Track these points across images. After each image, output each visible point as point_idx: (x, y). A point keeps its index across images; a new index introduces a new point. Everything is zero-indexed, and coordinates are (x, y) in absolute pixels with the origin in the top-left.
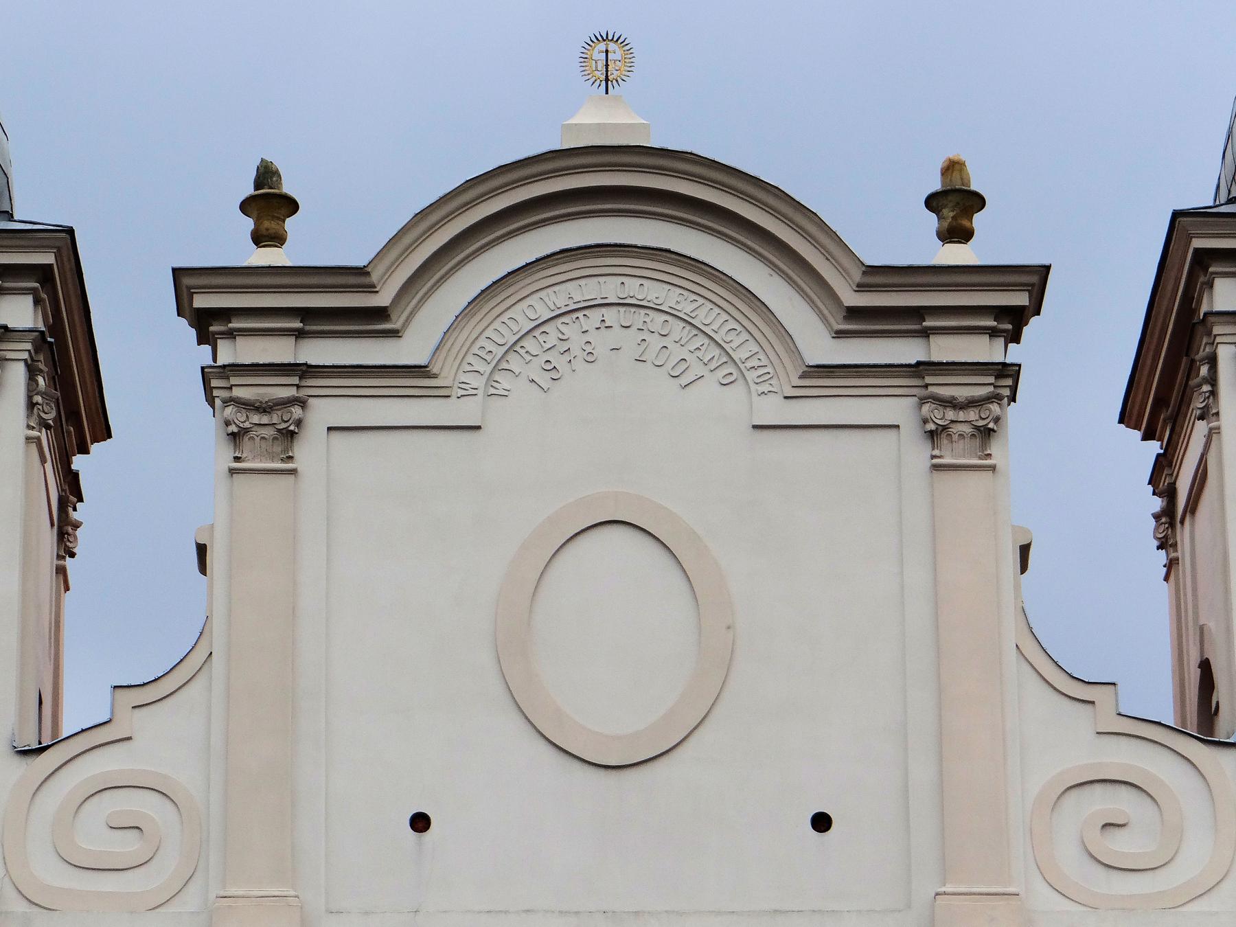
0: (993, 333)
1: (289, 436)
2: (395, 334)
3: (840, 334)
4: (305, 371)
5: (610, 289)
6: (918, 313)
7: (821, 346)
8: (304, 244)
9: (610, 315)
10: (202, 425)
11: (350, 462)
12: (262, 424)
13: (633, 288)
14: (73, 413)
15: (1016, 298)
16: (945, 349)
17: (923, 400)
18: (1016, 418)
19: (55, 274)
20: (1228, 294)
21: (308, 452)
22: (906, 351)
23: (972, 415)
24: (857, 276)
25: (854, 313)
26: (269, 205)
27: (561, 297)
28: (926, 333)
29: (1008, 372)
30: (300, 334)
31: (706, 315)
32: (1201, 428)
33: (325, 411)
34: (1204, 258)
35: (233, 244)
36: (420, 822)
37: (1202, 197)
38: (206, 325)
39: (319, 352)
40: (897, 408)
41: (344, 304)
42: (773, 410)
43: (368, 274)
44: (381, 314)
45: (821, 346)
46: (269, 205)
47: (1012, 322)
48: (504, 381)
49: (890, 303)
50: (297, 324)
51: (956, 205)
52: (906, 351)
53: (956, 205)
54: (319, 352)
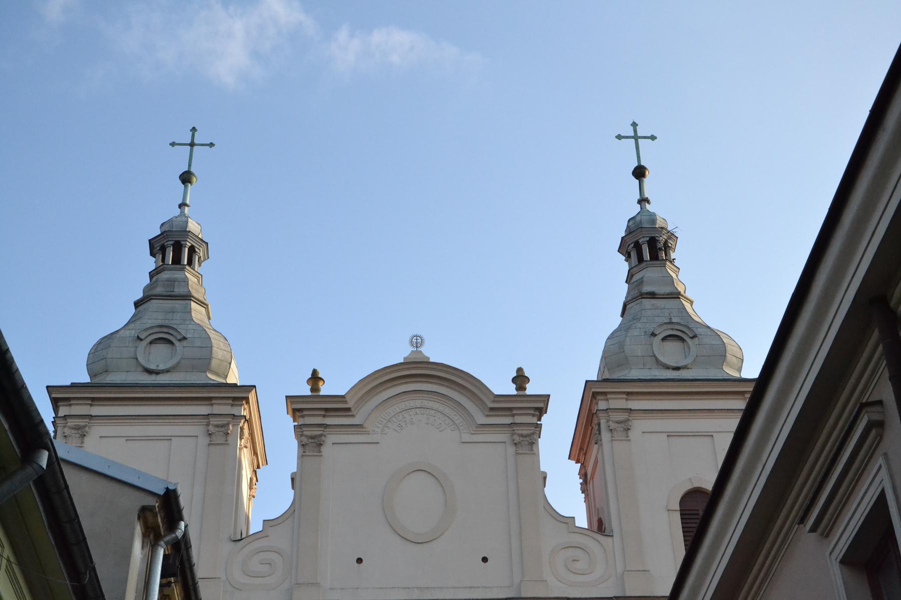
0: (533, 415)
1: (320, 445)
2: (353, 416)
3: (487, 416)
4: (326, 426)
5: (418, 403)
6: (510, 409)
7: (481, 419)
8: (325, 390)
9: (418, 411)
10: (292, 445)
11: (337, 452)
13: (426, 403)
15: (540, 406)
16: (518, 419)
17: (513, 435)
18: (541, 441)
20: (602, 405)
21: (326, 450)
23: (528, 439)
24: (492, 398)
25: (492, 409)
26: (315, 379)
28: (513, 415)
30: (324, 416)
31: (447, 411)
32: (596, 446)
33: (331, 438)
34: (595, 395)
36: (359, 561)
40: (504, 437)
41: (337, 406)
42: (466, 437)
43: (346, 402)
44: (349, 409)
45: (481, 419)
46: (315, 379)
48: (386, 430)
49: (501, 406)
50: (323, 413)
51: (520, 379)
52: (508, 420)
53: (520, 379)
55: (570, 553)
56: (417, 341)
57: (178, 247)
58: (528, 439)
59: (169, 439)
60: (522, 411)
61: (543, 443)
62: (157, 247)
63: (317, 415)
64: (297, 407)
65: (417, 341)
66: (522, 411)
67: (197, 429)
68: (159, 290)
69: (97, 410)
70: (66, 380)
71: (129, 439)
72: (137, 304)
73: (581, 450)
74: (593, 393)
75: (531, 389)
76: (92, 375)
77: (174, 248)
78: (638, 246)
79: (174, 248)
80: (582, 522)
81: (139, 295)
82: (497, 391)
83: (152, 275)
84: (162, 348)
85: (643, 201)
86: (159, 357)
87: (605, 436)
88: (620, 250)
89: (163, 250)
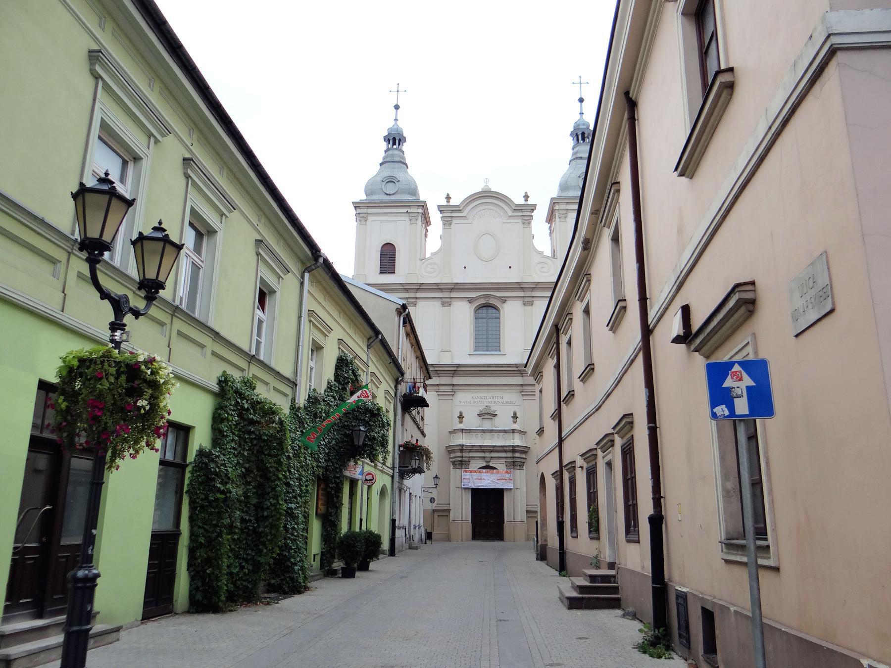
7: (510, 213)
8: (452, 203)
10: (441, 223)
11: (456, 225)
12: (447, 223)
14: (427, 222)
15: (533, 208)
16: (524, 214)
18: (533, 222)
19: (424, 206)
20: (557, 207)
21: (453, 226)
22: (520, 214)
26: (448, 198)
27: (481, 208)
29: (532, 216)
33: (454, 221)
35: (444, 203)
37: (555, 196)
38: (441, 211)
39: (453, 215)
40: (519, 220)
41: (456, 209)
42: (505, 221)
45: (510, 213)
46: (448, 198)
47: (533, 210)
49: (519, 208)
51: (526, 197)
52: (520, 214)
53: (526, 197)
54: (453, 215)
55: (542, 265)
56: (487, 181)
57: (394, 139)
58: (527, 222)
59: (396, 221)
60: (525, 211)
61: (534, 222)
62: (387, 139)
63: (450, 212)
64: (441, 209)
65: (487, 181)
66: (525, 211)
67: (406, 218)
68: (388, 159)
69: (370, 211)
70: (358, 200)
71: (382, 222)
72: (381, 164)
73: (550, 219)
74: (554, 202)
75: (530, 202)
76: (367, 195)
77: (395, 139)
78: (577, 135)
79: (395, 139)
80: (548, 252)
81: (381, 161)
82: (517, 203)
83: (385, 152)
84: (391, 184)
85: (582, 114)
86: (390, 189)
87: (557, 219)
88: (571, 135)
89: (389, 140)
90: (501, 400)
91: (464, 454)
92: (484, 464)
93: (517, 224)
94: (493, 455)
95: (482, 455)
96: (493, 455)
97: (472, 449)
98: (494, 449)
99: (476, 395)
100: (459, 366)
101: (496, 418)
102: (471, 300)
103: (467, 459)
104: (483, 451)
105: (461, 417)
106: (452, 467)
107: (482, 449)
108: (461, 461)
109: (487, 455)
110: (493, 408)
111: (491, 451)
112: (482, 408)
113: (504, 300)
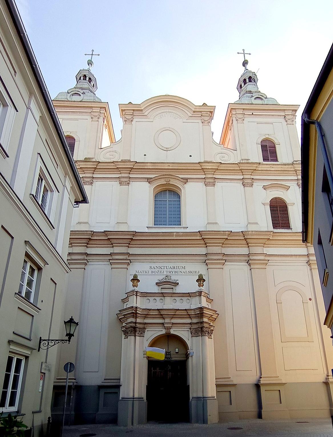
11: (138, 123)
25: (194, 112)
63: (130, 112)
87: (235, 122)
90: (183, 270)
91: (138, 320)
92: (164, 332)
93: (196, 124)
94: (174, 321)
95: (161, 321)
96: (174, 321)
97: (147, 313)
98: (175, 313)
99: (153, 265)
100: (135, 233)
101: (178, 286)
102: (149, 181)
103: (141, 326)
104: (162, 316)
105: (135, 279)
106: (123, 336)
107: (160, 313)
108: (135, 328)
109: (167, 320)
110: (174, 278)
111: (173, 317)
112: (161, 277)
113: (186, 181)
